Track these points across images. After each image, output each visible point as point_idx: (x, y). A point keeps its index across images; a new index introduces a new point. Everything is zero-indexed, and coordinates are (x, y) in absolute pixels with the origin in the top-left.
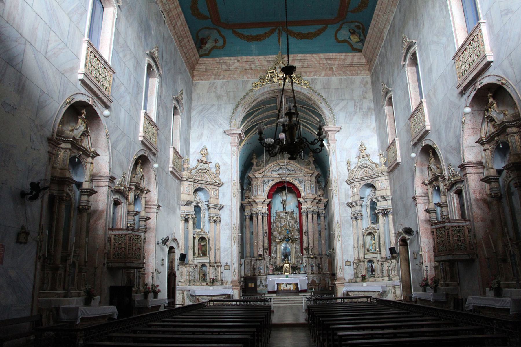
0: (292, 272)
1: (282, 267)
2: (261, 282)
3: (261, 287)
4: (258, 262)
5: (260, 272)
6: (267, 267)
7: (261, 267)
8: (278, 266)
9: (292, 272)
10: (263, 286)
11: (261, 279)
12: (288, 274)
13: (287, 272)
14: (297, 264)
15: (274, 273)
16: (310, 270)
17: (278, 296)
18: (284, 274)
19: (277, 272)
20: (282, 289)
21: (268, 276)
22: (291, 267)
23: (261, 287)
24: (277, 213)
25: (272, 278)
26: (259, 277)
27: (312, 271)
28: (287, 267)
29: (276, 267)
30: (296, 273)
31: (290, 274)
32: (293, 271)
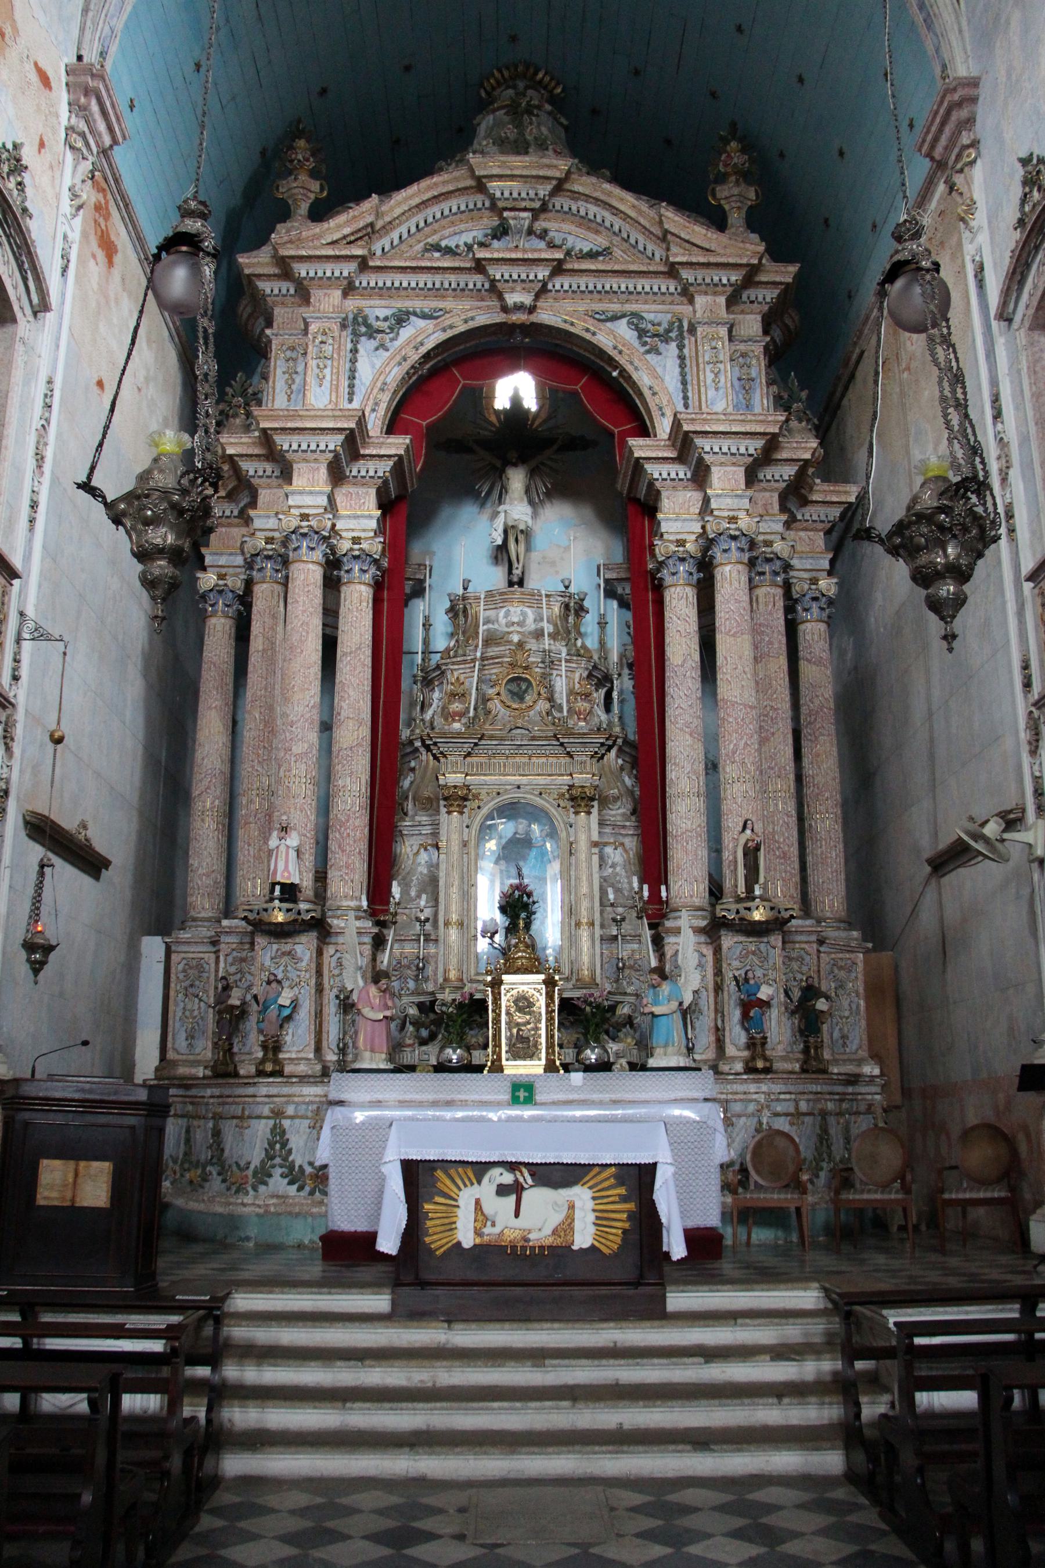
0: (569, 1055)
1: (480, 1006)
2: (279, 1137)
3: (278, 1183)
4: (266, 951)
5: (273, 1047)
6: (347, 1006)
7: (285, 999)
8: (447, 996)
9: (569, 1055)
10: (294, 1176)
11: (278, 1114)
12: (533, 1068)
13: (523, 1048)
14: (608, 987)
15: (408, 1057)
16: (736, 1037)
17: (415, 1315)
18: (497, 1068)
19: (431, 1054)
20: (467, 1238)
21: (342, 1086)
22: (567, 1007)
23: (278, 1183)
24: (458, 610)
25: (377, 1104)
26: (265, 1088)
27: (756, 1045)
28: (524, 1003)
29: (426, 1008)
30: (604, 1066)
31: (550, 1067)
32: (579, 1048)
